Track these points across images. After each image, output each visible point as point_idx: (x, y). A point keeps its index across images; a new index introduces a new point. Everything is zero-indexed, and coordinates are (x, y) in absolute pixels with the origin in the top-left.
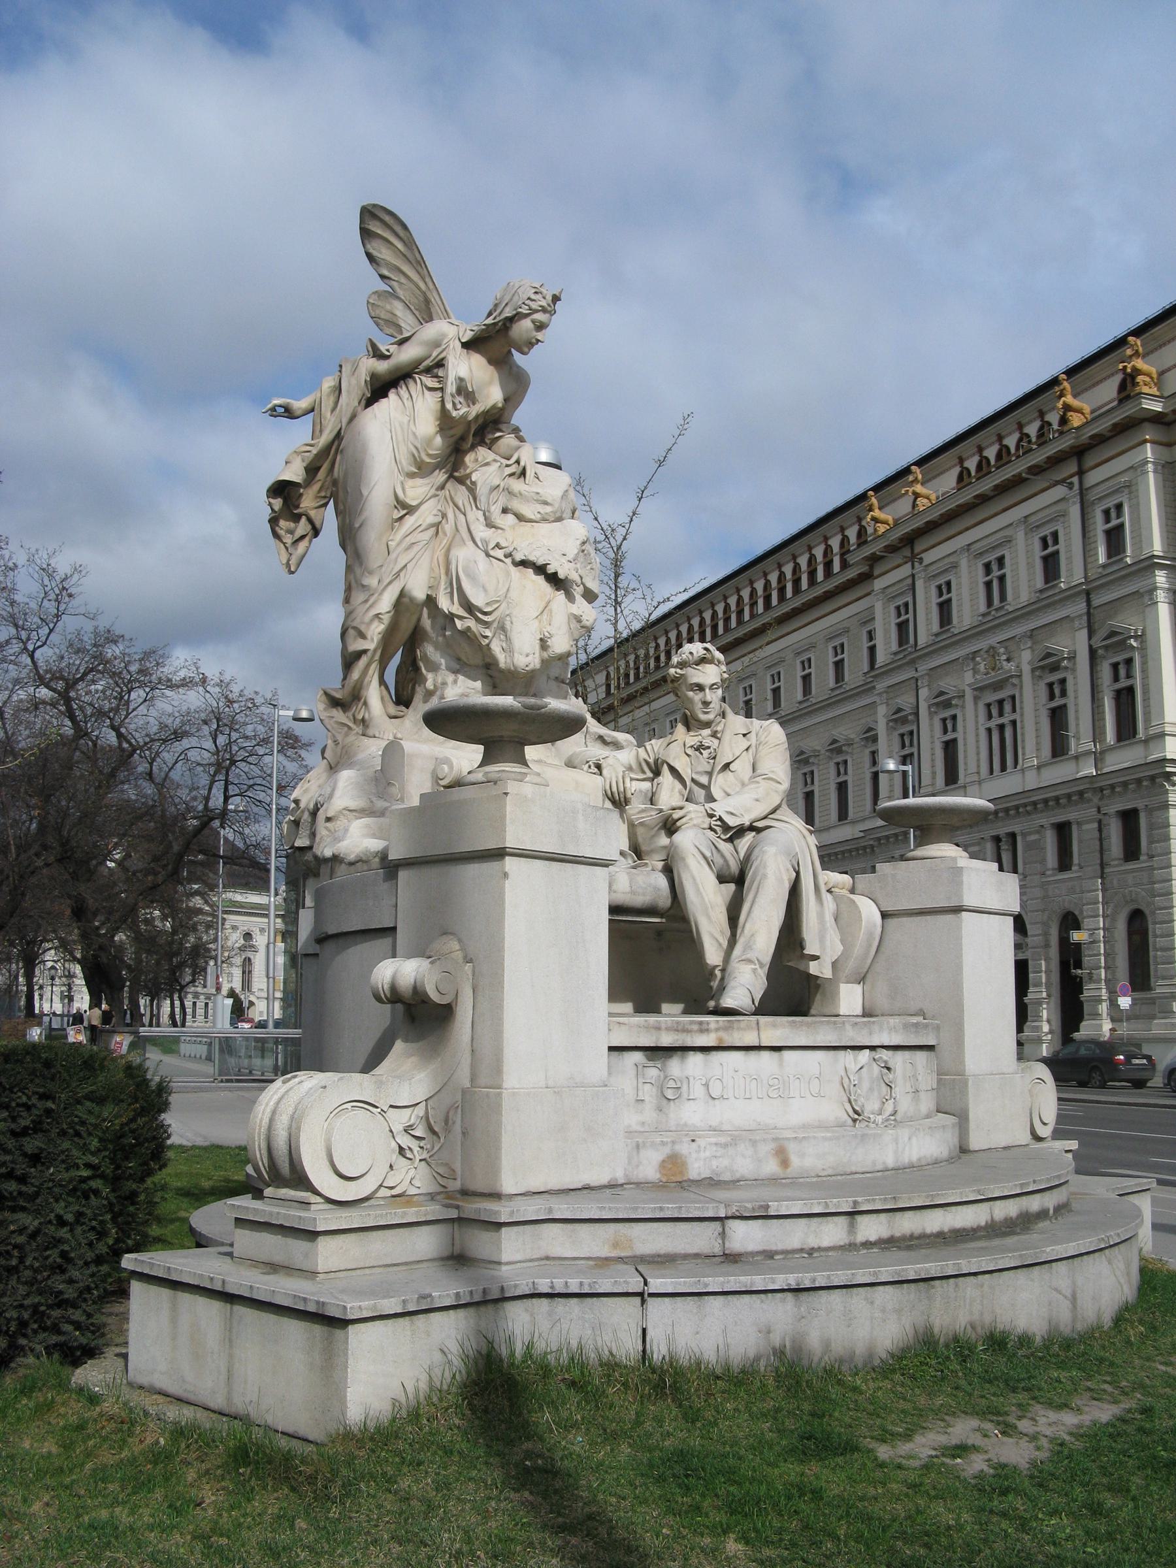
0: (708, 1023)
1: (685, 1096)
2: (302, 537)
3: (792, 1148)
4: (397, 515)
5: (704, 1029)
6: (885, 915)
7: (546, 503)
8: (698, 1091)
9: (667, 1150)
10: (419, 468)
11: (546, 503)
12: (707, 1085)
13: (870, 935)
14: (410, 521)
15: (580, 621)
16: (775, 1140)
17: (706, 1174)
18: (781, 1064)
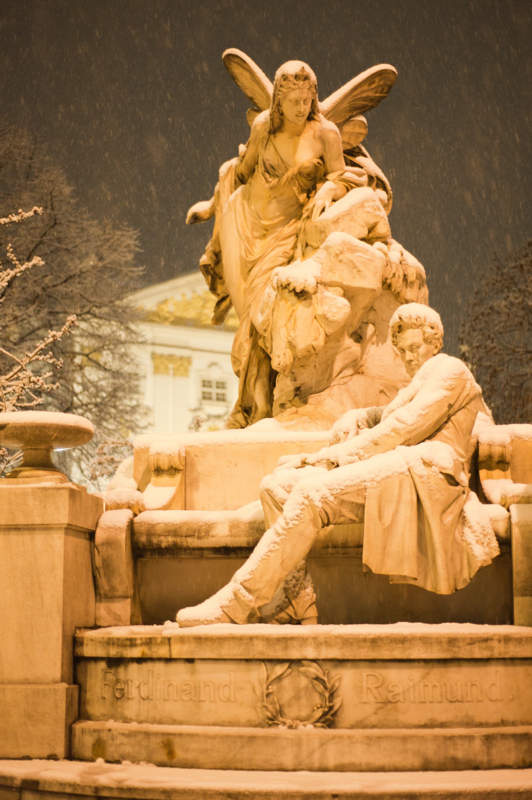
3: (177, 741)
8: (133, 692)
10: (266, 230)
12: (139, 687)
15: (327, 319)
16: (163, 734)
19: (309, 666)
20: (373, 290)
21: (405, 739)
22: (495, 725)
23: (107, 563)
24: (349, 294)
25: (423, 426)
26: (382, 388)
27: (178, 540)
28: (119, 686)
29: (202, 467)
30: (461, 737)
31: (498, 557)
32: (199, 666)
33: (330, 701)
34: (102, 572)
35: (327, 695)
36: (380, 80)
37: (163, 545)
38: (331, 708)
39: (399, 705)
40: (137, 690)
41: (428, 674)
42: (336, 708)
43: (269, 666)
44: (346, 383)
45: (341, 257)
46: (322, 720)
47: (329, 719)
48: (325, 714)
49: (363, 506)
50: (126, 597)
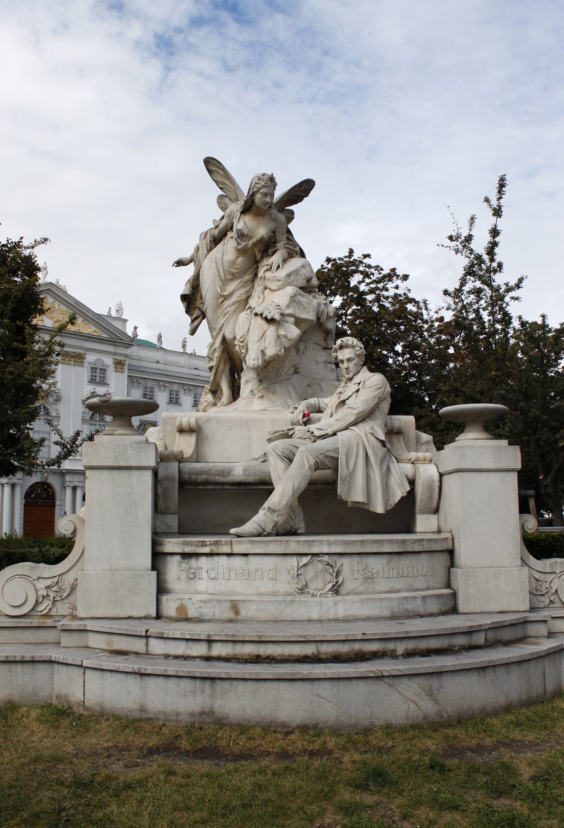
0: (205, 542)
1: (197, 577)
2: (196, 318)
3: (240, 605)
4: (220, 301)
5: (203, 544)
6: (441, 475)
7: (279, 281)
8: (204, 575)
9: (179, 603)
10: (234, 276)
11: (279, 281)
12: (207, 571)
13: (430, 488)
14: (227, 303)
15: (286, 338)
16: (231, 601)
17: (196, 615)
18: (247, 563)
19: (323, 557)
20: (312, 321)
21: (382, 599)
22: (423, 590)
23: (165, 492)
24: (298, 322)
25: (366, 410)
26: (308, 383)
27: (209, 477)
28: (192, 571)
29: (208, 429)
30: (411, 597)
31: (409, 491)
32: (251, 558)
33: (336, 579)
34: (161, 497)
35: (335, 575)
36: (306, 185)
37: (199, 480)
38: (337, 582)
39: (375, 579)
40: (206, 573)
41: (390, 561)
42: (340, 582)
43: (299, 558)
44: (289, 379)
45: (294, 299)
46: (332, 590)
47: (336, 590)
48: (333, 586)
49: (338, 459)
50: (175, 514)
